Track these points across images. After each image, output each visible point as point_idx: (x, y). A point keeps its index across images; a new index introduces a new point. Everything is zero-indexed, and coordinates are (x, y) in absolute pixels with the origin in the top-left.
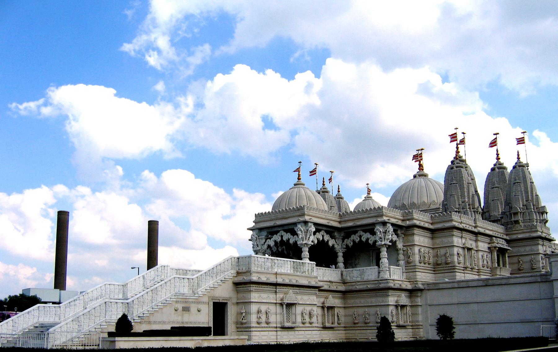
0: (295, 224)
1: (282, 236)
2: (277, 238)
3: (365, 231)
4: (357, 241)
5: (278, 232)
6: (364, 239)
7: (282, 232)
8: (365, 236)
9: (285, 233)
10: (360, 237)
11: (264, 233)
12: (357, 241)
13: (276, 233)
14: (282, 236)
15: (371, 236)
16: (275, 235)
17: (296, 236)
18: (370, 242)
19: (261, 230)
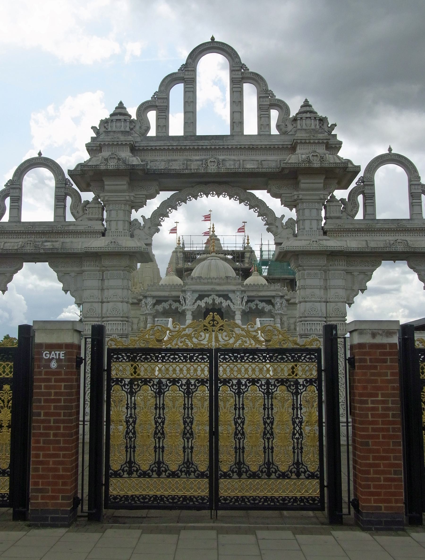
0: (234, 291)
1: (214, 300)
2: (209, 300)
3: (262, 301)
4: (254, 308)
5: (210, 295)
6: (260, 308)
7: (215, 296)
8: (261, 305)
9: (218, 297)
10: (257, 305)
11: (196, 295)
12: (254, 308)
13: (208, 296)
14: (214, 300)
15: (267, 305)
16: (206, 299)
17: (229, 301)
18: (265, 310)
19: (194, 291)
